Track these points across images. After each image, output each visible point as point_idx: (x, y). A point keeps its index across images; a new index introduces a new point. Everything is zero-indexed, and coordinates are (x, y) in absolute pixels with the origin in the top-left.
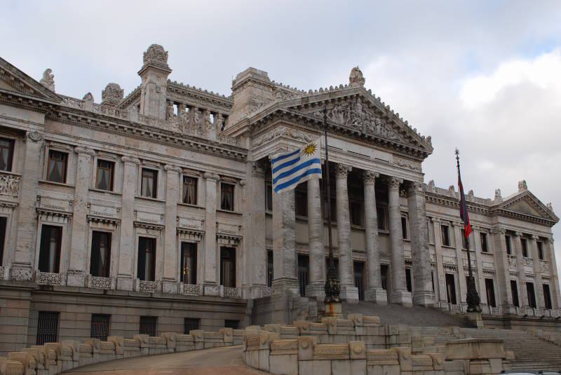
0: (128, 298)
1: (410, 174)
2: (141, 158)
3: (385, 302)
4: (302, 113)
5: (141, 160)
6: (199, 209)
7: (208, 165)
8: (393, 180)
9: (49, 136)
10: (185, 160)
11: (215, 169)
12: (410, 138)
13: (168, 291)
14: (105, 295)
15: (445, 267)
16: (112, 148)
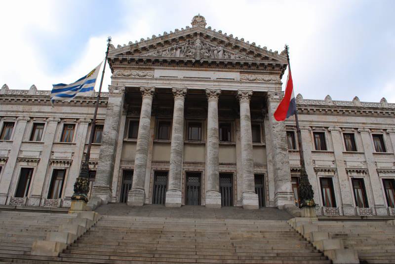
1: (265, 85)
2: (31, 116)
3: (219, 205)
4: (136, 57)
5: (32, 118)
6: (72, 145)
7: (83, 114)
8: (240, 93)
10: (63, 113)
11: (88, 116)
12: (259, 55)
13: (32, 204)
15: (348, 171)
16: (12, 113)
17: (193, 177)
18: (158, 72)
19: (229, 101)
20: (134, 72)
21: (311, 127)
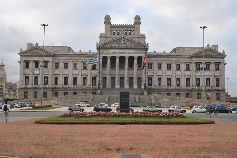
0: (70, 89)
4: (105, 46)
9: (54, 60)
14: (66, 88)
17: (122, 79)
18: (112, 51)
19: (131, 59)
20: (105, 51)
21: (157, 62)
